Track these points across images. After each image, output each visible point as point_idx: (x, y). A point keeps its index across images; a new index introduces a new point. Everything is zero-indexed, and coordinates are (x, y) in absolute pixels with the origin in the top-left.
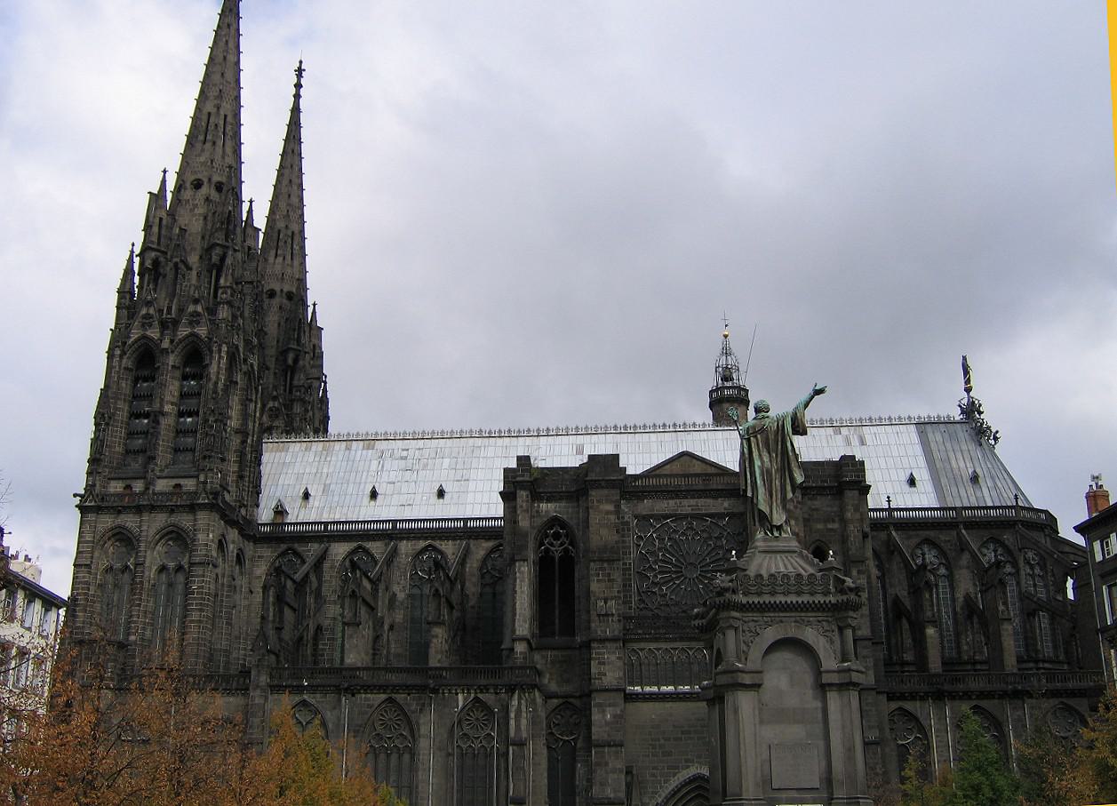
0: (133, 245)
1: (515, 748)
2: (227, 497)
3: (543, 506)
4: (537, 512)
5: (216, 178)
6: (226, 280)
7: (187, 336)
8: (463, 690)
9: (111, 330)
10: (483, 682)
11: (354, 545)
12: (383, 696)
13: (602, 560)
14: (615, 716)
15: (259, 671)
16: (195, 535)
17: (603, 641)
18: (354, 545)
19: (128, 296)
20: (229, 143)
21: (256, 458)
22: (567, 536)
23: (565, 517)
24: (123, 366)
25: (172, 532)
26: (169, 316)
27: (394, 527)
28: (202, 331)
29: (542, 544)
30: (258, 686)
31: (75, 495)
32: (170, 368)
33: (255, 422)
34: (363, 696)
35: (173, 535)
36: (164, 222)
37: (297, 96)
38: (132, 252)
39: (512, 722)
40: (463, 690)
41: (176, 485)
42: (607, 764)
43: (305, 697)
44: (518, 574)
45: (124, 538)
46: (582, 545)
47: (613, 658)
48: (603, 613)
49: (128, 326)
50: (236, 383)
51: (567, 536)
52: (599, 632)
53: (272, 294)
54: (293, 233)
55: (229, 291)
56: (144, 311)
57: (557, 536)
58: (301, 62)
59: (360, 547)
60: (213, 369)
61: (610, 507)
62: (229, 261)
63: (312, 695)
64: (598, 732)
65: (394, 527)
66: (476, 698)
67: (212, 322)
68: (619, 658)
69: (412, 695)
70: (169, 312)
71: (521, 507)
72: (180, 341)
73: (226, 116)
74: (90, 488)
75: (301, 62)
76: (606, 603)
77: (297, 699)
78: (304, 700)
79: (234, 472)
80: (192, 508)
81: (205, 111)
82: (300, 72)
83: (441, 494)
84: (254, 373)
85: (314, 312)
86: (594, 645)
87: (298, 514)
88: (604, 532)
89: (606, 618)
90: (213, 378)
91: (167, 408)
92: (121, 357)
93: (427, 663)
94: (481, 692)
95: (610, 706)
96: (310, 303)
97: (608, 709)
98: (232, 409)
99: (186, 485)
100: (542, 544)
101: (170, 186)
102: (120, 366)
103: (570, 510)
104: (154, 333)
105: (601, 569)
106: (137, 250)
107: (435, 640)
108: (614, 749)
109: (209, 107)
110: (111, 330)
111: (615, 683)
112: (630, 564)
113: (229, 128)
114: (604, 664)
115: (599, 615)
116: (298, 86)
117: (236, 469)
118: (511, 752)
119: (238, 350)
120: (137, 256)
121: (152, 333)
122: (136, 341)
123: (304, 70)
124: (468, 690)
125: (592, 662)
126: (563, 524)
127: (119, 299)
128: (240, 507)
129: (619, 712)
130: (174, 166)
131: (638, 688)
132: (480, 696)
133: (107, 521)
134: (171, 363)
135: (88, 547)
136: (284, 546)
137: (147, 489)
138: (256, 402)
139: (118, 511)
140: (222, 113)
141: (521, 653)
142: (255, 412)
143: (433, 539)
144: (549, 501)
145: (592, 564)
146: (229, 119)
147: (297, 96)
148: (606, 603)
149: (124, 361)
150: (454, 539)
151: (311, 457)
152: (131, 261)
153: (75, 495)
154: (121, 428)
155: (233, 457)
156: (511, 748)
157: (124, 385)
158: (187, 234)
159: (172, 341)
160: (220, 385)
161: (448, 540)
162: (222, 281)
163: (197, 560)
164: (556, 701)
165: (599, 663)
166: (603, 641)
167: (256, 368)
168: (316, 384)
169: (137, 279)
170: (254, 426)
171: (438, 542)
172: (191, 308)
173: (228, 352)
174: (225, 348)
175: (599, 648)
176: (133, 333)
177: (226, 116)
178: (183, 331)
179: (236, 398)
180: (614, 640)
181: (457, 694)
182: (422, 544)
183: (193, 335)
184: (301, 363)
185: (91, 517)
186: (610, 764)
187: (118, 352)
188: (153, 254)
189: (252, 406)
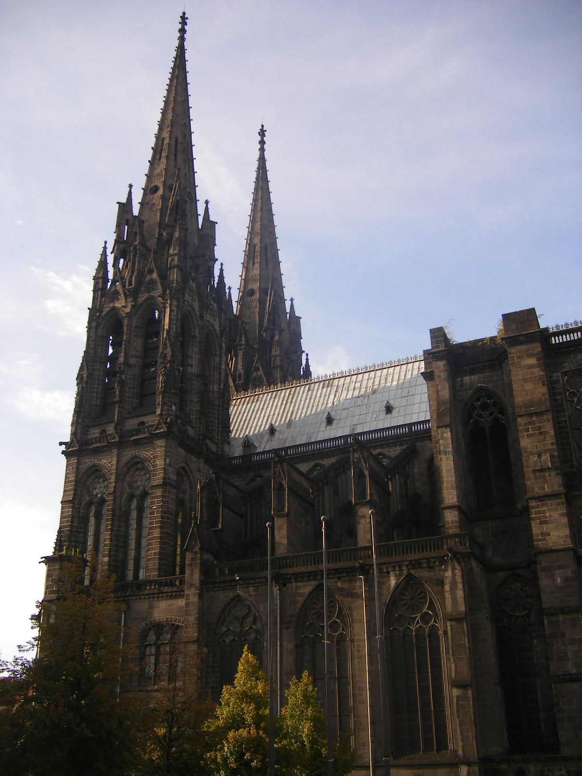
0: (106, 243)
1: (453, 623)
2: (191, 432)
3: (467, 379)
4: (462, 385)
5: (169, 182)
6: (174, 250)
7: (145, 300)
8: (394, 567)
9: (89, 309)
10: (413, 556)
11: (311, 464)
13: (531, 415)
14: (566, 579)
15: (192, 570)
16: (154, 462)
17: (542, 498)
18: (311, 464)
19: (101, 281)
20: (179, 157)
21: (223, 402)
22: (495, 405)
23: (490, 385)
24: (99, 334)
25: (138, 463)
26: (130, 287)
27: (346, 442)
29: (471, 417)
30: (191, 585)
31: (61, 444)
32: (133, 329)
33: (220, 372)
34: (294, 585)
35: (139, 465)
36: (130, 223)
37: (262, 150)
38: (105, 248)
39: (447, 595)
40: (394, 567)
41: (141, 422)
42: (563, 635)
43: (239, 592)
44: (441, 442)
45: (96, 472)
46: (510, 408)
47: (556, 515)
48: (538, 468)
50: (195, 337)
51: (495, 405)
52: (536, 490)
54: (266, 246)
55: (176, 258)
56: (113, 289)
57: (485, 407)
58: (263, 126)
59: (317, 465)
61: (532, 361)
62: (177, 235)
63: (245, 590)
64: (548, 600)
65: (346, 442)
66: (409, 575)
67: (163, 285)
68: (562, 515)
69: (342, 579)
70: (130, 284)
71: (440, 377)
72: (141, 305)
73: (176, 139)
74: (74, 434)
75: (263, 126)
76: (540, 457)
77: (231, 594)
78: (239, 595)
79: (197, 411)
81: (161, 139)
83: (389, 409)
84: (216, 333)
85: (292, 306)
86: (532, 503)
87: (264, 446)
88: (529, 386)
89: (541, 474)
90: (166, 327)
91: (133, 361)
92: (97, 328)
93: (356, 543)
94: (414, 568)
95: (559, 569)
96: (287, 295)
97: (557, 572)
98: (192, 358)
99: (148, 422)
100: (471, 417)
102: (96, 335)
103: (495, 378)
105: (530, 423)
107: (362, 521)
108: (569, 617)
109: (166, 134)
110: (89, 309)
111: (561, 542)
112: (565, 422)
113: (179, 146)
114: (546, 522)
115: (534, 471)
116: (262, 143)
117: (199, 408)
118: (449, 628)
119: (193, 309)
120: (112, 253)
121: (119, 304)
122: (108, 313)
123: (265, 131)
124: (400, 566)
125: (532, 523)
126: (489, 394)
128: (204, 440)
129: (570, 575)
130: (140, 183)
132: (412, 572)
133: (88, 462)
134: (134, 325)
135: (71, 486)
136: (252, 474)
137: (116, 428)
138: (220, 356)
139: (97, 451)
140: (173, 135)
141: (452, 522)
142: (220, 365)
143: (382, 446)
144: (472, 373)
145: (519, 419)
146: (180, 140)
148: (540, 457)
149: (100, 330)
150: (401, 445)
151: (278, 402)
152: (104, 254)
153: (61, 444)
154: (98, 384)
155: (195, 399)
156: (448, 623)
157: (100, 350)
158: (145, 225)
159: (133, 307)
160: (172, 334)
161: (396, 446)
162: (171, 251)
163: (156, 483)
164: (501, 575)
165: (541, 523)
166: (542, 498)
167: (217, 328)
170: (220, 376)
171: (387, 449)
172: (148, 278)
173: (178, 306)
174: (175, 303)
175: (538, 506)
176: (105, 308)
177: (176, 139)
178: (143, 297)
181: (388, 573)
184: (277, 338)
185: (74, 460)
186: (567, 635)
187: (94, 324)
188: (122, 246)
189: (217, 359)
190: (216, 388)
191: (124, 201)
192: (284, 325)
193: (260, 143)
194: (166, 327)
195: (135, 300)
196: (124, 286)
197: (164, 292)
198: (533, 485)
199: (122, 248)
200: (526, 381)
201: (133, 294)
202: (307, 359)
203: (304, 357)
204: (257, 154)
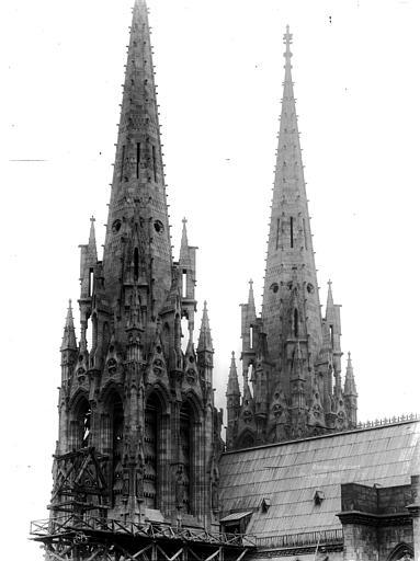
28: (116, 377)
37: (288, 67)
58: (288, 27)
75: (288, 27)
82: (288, 38)
101: (101, 237)
116: (288, 55)
122: (77, 393)
130: (103, 216)
147: (288, 67)
152: (70, 317)
179: (169, 431)
183: (111, 382)
190: (201, 463)
191: (86, 243)
193: (285, 55)
202: (349, 360)
204: (281, 77)
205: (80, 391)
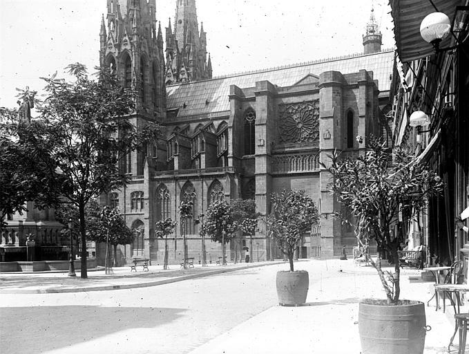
12: (186, 180)
17: (259, 156)
28: (128, 47)
49: (105, 49)
53: (180, 22)
57: (251, 115)
60: (133, 62)
80: (132, 117)
96: (199, 22)
104: (113, 50)
106: (105, 16)
127: (101, 38)
131: (276, 173)
159: (119, 53)
166: (259, 156)
168: (201, 57)
169: (107, 29)
178: (123, 48)
180: (263, 155)
182: (221, 121)
192: (196, 40)
194: (134, 66)
195: (119, 50)
196: (114, 41)
197: (132, 47)
198: (258, 151)
199: (111, 18)
200: (260, 108)
201: (118, 46)
203: (207, 55)
205: (110, 53)
